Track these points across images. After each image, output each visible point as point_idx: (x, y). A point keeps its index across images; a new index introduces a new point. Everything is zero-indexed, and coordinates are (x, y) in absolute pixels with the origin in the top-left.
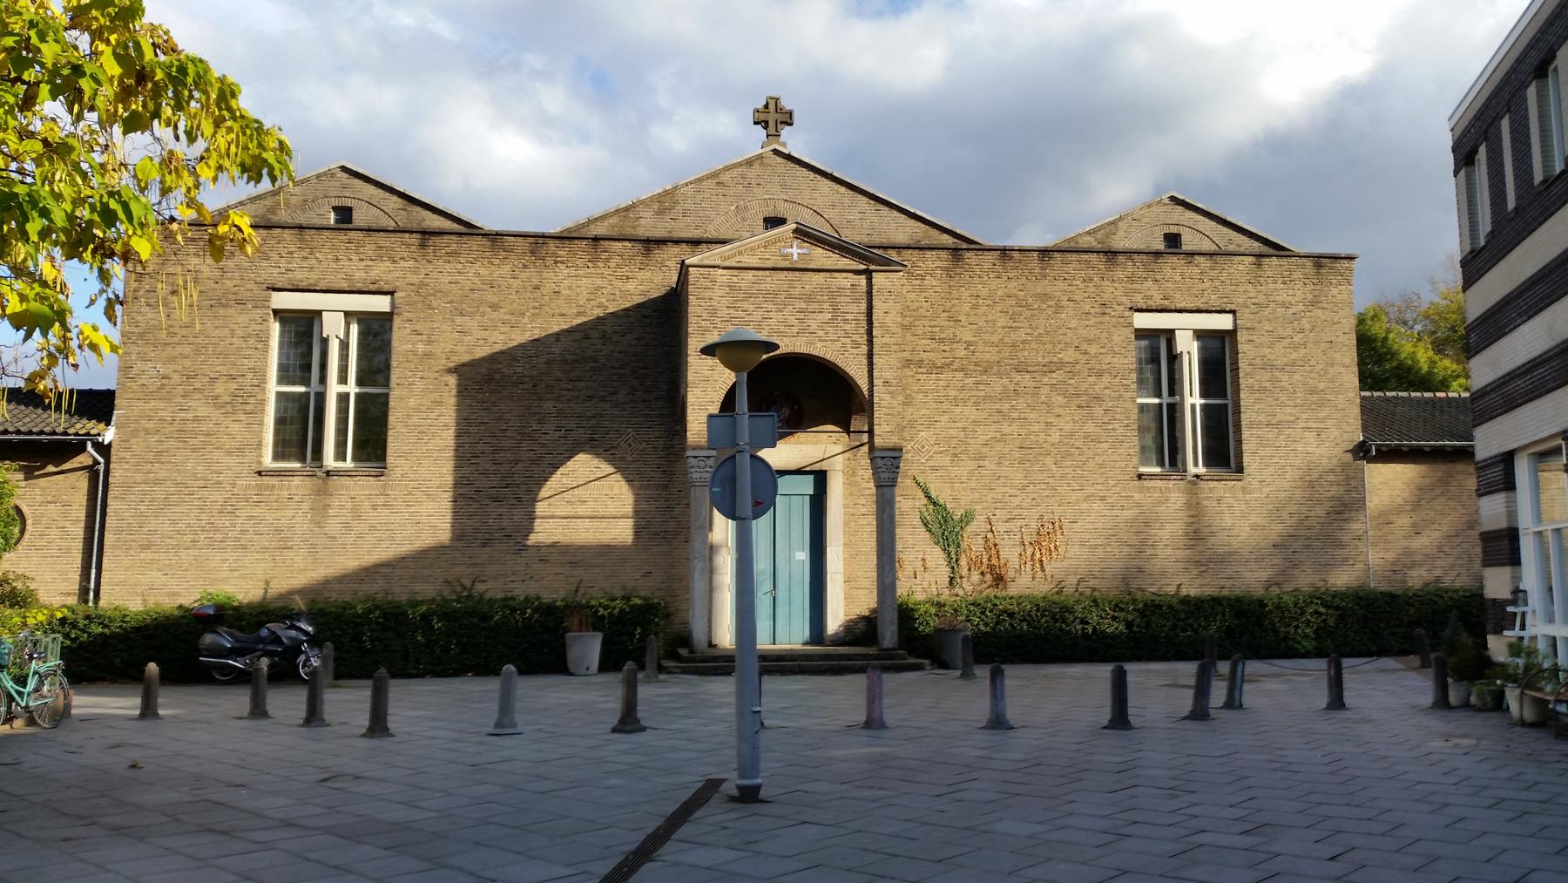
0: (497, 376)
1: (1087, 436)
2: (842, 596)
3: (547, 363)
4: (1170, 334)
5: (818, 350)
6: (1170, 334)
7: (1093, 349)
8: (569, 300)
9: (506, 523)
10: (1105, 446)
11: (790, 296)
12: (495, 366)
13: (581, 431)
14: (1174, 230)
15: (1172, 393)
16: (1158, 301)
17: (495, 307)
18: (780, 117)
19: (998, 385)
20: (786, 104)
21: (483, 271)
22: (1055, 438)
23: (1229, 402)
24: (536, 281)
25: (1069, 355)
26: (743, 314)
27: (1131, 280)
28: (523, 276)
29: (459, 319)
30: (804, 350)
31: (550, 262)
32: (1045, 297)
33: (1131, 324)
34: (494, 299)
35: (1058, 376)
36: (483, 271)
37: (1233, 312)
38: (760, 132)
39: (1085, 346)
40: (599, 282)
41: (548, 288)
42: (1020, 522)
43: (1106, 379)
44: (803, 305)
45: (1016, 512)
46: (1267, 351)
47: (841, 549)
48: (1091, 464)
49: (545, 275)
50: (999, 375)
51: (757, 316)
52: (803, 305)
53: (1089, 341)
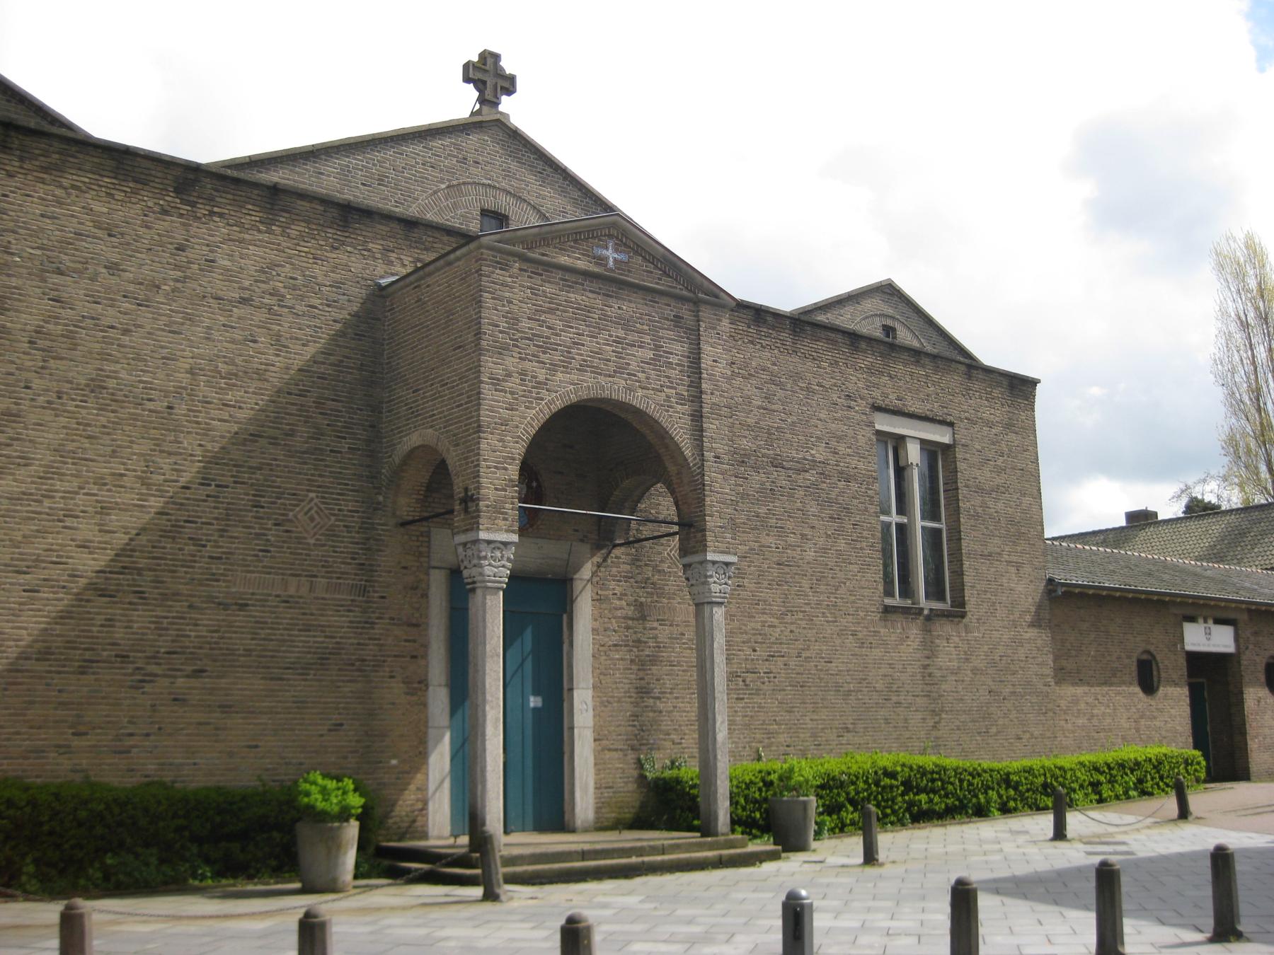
0: (111, 383)
1: (839, 553)
2: (591, 760)
3: (191, 372)
4: (899, 442)
5: (638, 399)
6: (899, 442)
7: (842, 448)
8: (228, 275)
9: (119, 633)
10: (855, 568)
11: (604, 317)
12: (109, 367)
13: (240, 489)
14: (889, 322)
15: (901, 511)
16: (892, 401)
17: (113, 268)
18: (501, 83)
19: (757, 479)
20: (508, 66)
21: (98, 207)
22: (810, 555)
23: (942, 525)
24: (179, 237)
25: (819, 453)
26: (546, 332)
27: (870, 370)
28: (162, 225)
29: (56, 279)
30: (622, 397)
31: (202, 210)
32: (796, 377)
33: (871, 424)
34: (115, 258)
35: (811, 476)
36: (98, 207)
37: (951, 424)
38: (471, 93)
39: (833, 443)
40: (272, 256)
41: (197, 252)
42: (780, 661)
43: (854, 486)
44: (621, 333)
45: (775, 648)
46: (978, 473)
47: (590, 693)
48: (843, 590)
49: (193, 230)
50: (756, 469)
51: (566, 338)
52: (621, 333)
53: (840, 439)
